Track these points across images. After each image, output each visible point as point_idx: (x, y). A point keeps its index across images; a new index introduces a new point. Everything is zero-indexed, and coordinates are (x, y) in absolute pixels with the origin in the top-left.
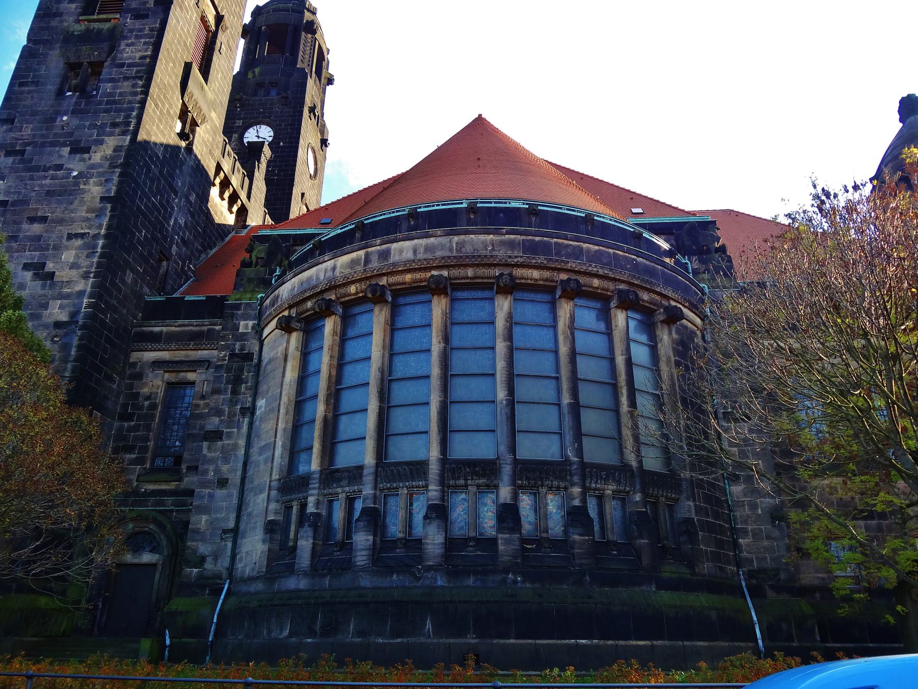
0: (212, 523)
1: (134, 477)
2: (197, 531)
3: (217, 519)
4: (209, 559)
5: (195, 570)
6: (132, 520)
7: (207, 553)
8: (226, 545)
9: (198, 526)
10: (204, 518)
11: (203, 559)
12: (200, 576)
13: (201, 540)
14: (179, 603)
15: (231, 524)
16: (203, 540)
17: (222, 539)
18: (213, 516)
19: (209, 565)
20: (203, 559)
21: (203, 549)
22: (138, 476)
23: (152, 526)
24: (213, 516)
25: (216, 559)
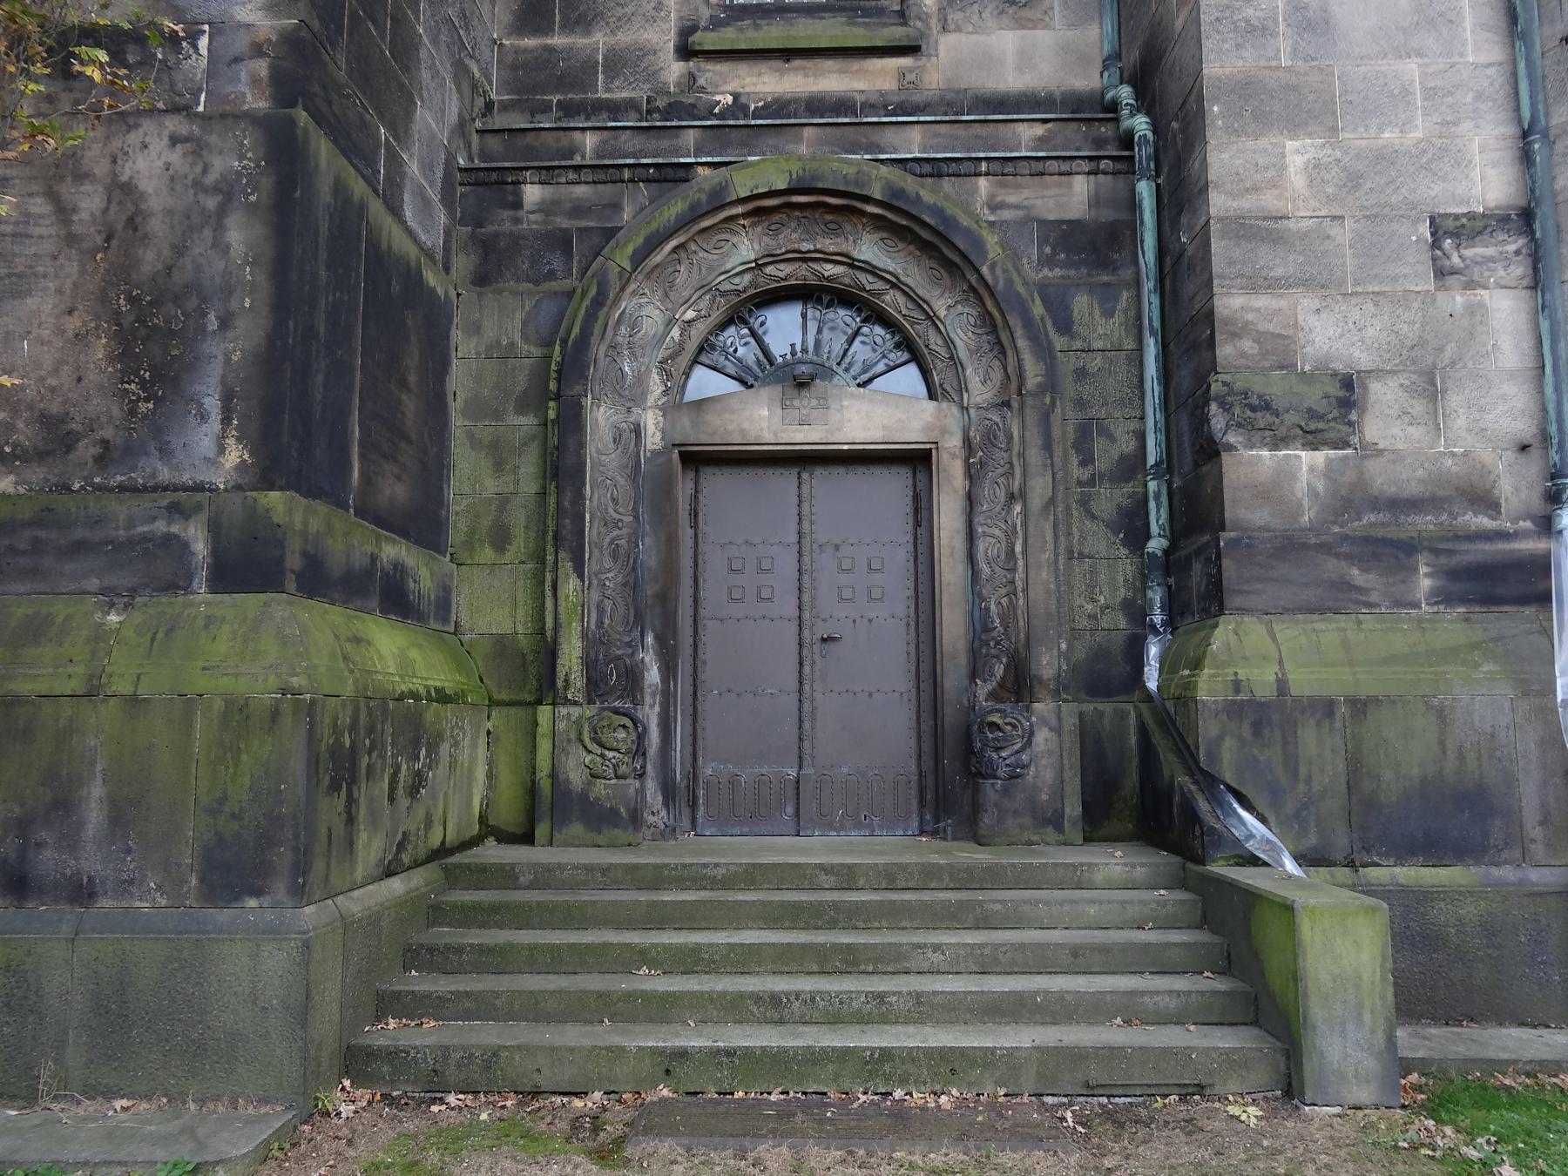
0: (1353, 180)
1: (663, 37)
2: (1262, 230)
3: (1383, 157)
4: (1384, 395)
5: (1309, 462)
6: (764, 210)
7: (1363, 359)
8: (1475, 311)
9: (1269, 201)
10: (1298, 153)
11: (1347, 393)
12: (1349, 499)
13: (1306, 283)
14: (1257, 650)
15: (1488, 182)
16: (1322, 284)
17: (1441, 273)
18: (1357, 138)
19: (1390, 423)
20: (1347, 393)
21: (1329, 333)
22: (686, 32)
23: (869, 249)
24: (1357, 138)
25: (1430, 389)
